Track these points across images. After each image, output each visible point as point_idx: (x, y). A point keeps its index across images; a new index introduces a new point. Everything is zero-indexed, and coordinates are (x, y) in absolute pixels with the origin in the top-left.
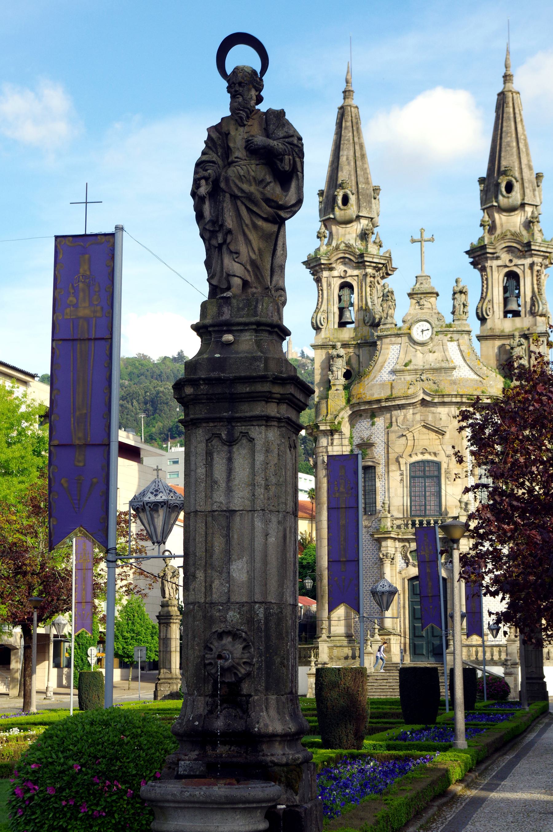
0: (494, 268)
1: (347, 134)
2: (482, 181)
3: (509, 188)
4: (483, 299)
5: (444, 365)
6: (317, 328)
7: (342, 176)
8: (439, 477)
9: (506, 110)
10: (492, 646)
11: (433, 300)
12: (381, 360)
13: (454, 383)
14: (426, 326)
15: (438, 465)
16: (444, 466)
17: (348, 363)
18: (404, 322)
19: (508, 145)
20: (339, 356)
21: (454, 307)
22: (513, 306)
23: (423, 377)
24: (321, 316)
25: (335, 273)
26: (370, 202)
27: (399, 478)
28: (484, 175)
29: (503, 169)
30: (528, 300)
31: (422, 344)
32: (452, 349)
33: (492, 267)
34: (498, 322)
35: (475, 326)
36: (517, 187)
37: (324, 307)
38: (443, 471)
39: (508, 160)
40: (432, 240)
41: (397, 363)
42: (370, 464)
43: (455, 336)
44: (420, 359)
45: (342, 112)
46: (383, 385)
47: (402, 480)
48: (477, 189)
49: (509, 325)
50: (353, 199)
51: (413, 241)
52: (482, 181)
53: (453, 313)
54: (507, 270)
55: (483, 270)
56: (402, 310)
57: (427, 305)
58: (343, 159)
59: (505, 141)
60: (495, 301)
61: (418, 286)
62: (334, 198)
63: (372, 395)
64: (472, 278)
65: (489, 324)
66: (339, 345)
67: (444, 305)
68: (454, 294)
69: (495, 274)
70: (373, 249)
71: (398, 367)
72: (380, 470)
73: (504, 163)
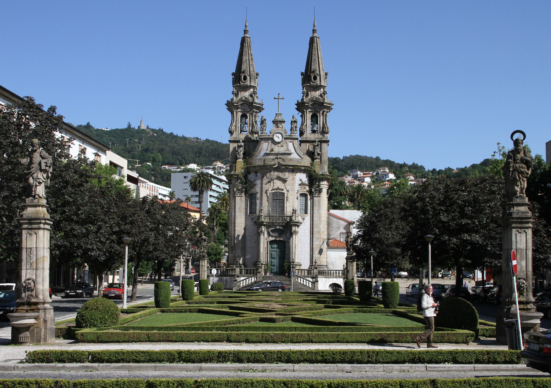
1: (245, 49)
2: (302, 74)
3: (315, 78)
4: (302, 124)
5: (287, 152)
6: (231, 133)
7: (244, 67)
8: (284, 200)
9: (314, 45)
10: (298, 270)
11: (283, 124)
13: (291, 160)
14: (280, 136)
15: (284, 193)
16: (286, 195)
17: (245, 149)
18: (270, 133)
19: (315, 59)
20: (241, 146)
21: (292, 127)
22: (315, 129)
23: (278, 157)
24: (233, 128)
26: (255, 80)
28: (304, 71)
29: (312, 70)
30: (321, 126)
31: (279, 143)
32: (290, 145)
34: (308, 135)
36: (318, 77)
37: (234, 124)
39: (314, 66)
40: (283, 99)
41: (267, 150)
43: (292, 141)
44: (277, 149)
45: (243, 40)
48: (300, 78)
49: (312, 137)
50: (248, 77)
51: (275, 98)
53: (291, 130)
55: (303, 113)
56: (270, 127)
57: (281, 126)
58: (244, 60)
59: (313, 58)
61: (277, 118)
62: (240, 77)
63: (255, 163)
64: (298, 116)
65: (305, 135)
66: (241, 141)
67: (287, 126)
68: (292, 122)
69: (308, 114)
70: (256, 101)
71: (267, 152)
72: (258, 196)
73: (313, 67)
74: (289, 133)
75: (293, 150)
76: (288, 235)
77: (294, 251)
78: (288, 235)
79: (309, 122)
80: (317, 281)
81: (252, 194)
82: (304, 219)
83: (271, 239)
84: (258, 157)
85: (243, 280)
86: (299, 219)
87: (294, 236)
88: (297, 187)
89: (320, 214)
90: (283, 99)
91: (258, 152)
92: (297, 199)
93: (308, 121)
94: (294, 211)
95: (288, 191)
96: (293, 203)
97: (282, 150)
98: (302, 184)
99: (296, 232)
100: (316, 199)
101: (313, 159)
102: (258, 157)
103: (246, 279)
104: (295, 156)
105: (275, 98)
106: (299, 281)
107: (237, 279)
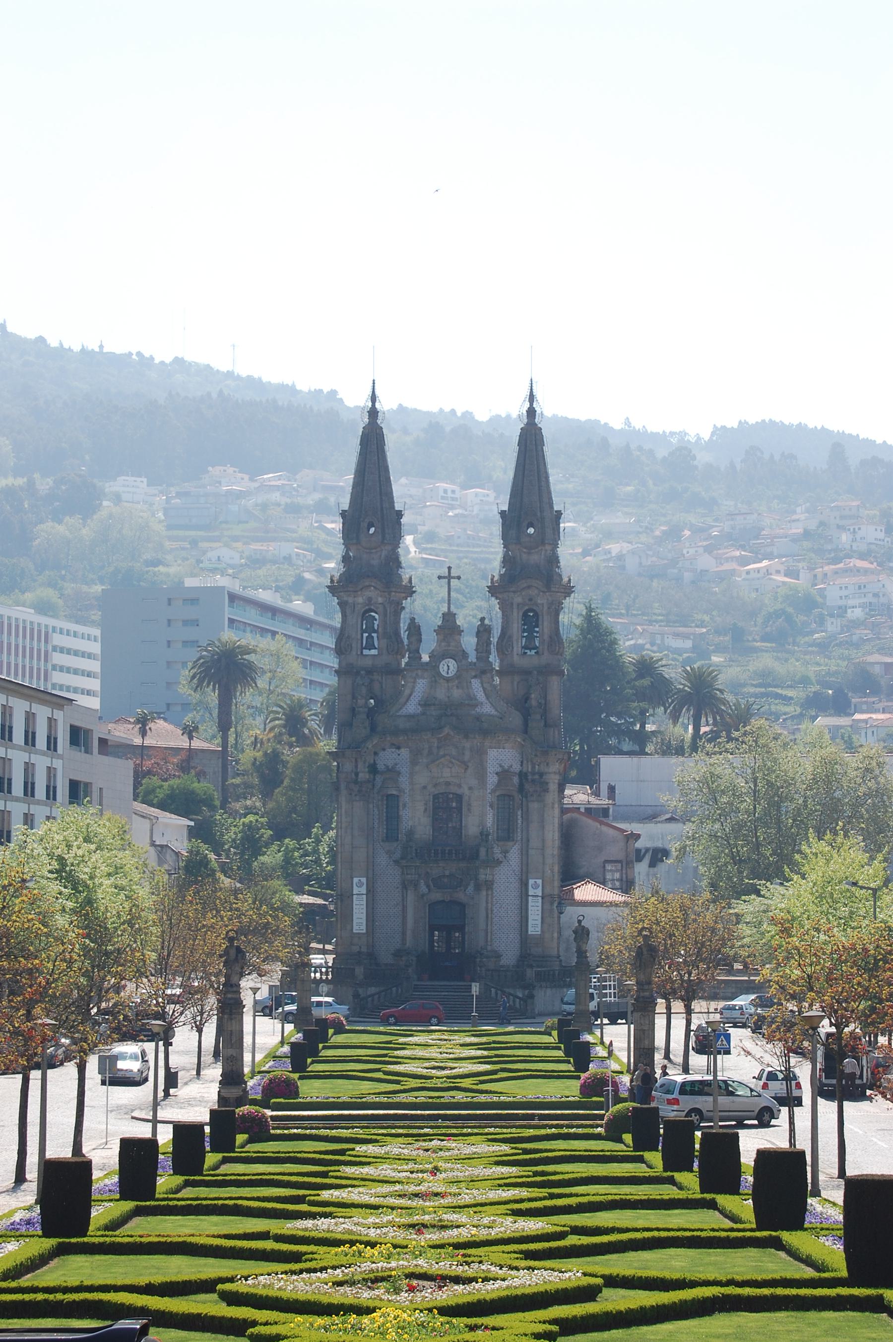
0: (515, 606)
2: (502, 513)
12: (407, 692)
15: (459, 798)
16: (465, 798)
25: (360, 600)
27: (422, 808)
28: (505, 508)
33: (512, 604)
35: (495, 660)
38: (464, 804)
42: (395, 793)
46: (410, 717)
47: (426, 810)
52: (502, 513)
54: (527, 608)
60: (515, 638)
67: (469, 642)
69: (515, 611)
74: (472, 658)
75: (481, 696)
76: (471, 889)
77: (482, 925)
78: (471, 889)
79: (516, 626)
80: (532, 997)
81: (389, 796)
82: (505, 852)
83: (437, 896)
84: (404, 711)
85: (372, 995)
86: (497, 852)
87: (484, 893)
88: (492, 780)
89: (543, 840)
90: (459, 578)
91: (402, 700)
92: (491, 806)
93: (515, 625)
94: (484, 835)
95: (470, 788)
96: (480, 817)
97: (456, 693)
98: (504, 774)
99: (489, 885)
100: (534, 806)
101: (526, 714)
102: (404, 711)
103: (379, 993)
104: (487, 709)
105: (440, 577)
106: (493, 994)
107: (360, 991)
